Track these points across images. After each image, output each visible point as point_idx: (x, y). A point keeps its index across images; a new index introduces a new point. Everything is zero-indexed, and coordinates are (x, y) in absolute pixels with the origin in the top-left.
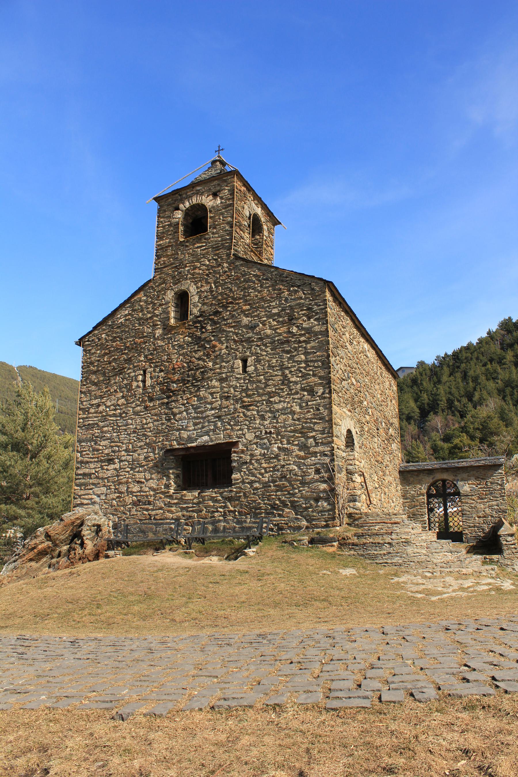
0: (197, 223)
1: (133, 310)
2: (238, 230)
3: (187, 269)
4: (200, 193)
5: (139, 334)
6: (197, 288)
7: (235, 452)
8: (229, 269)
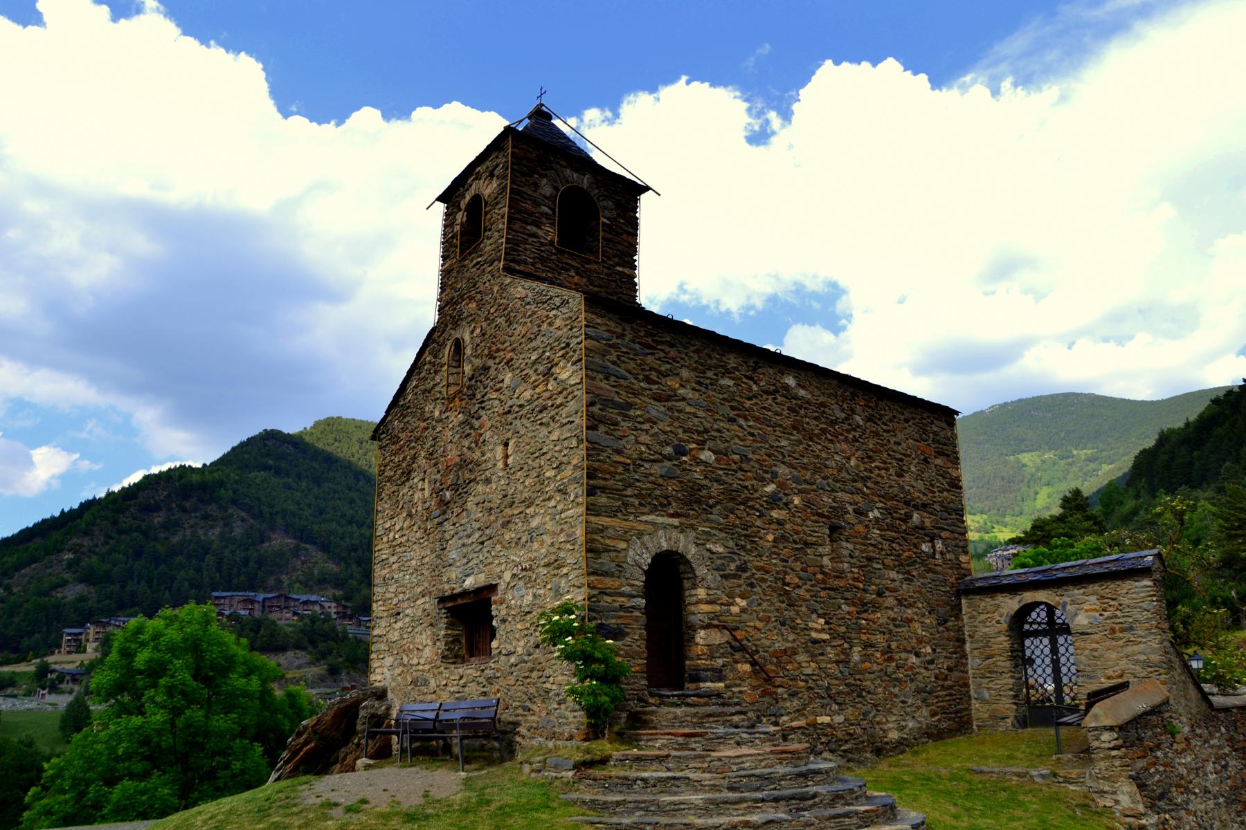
7: (495, 603)
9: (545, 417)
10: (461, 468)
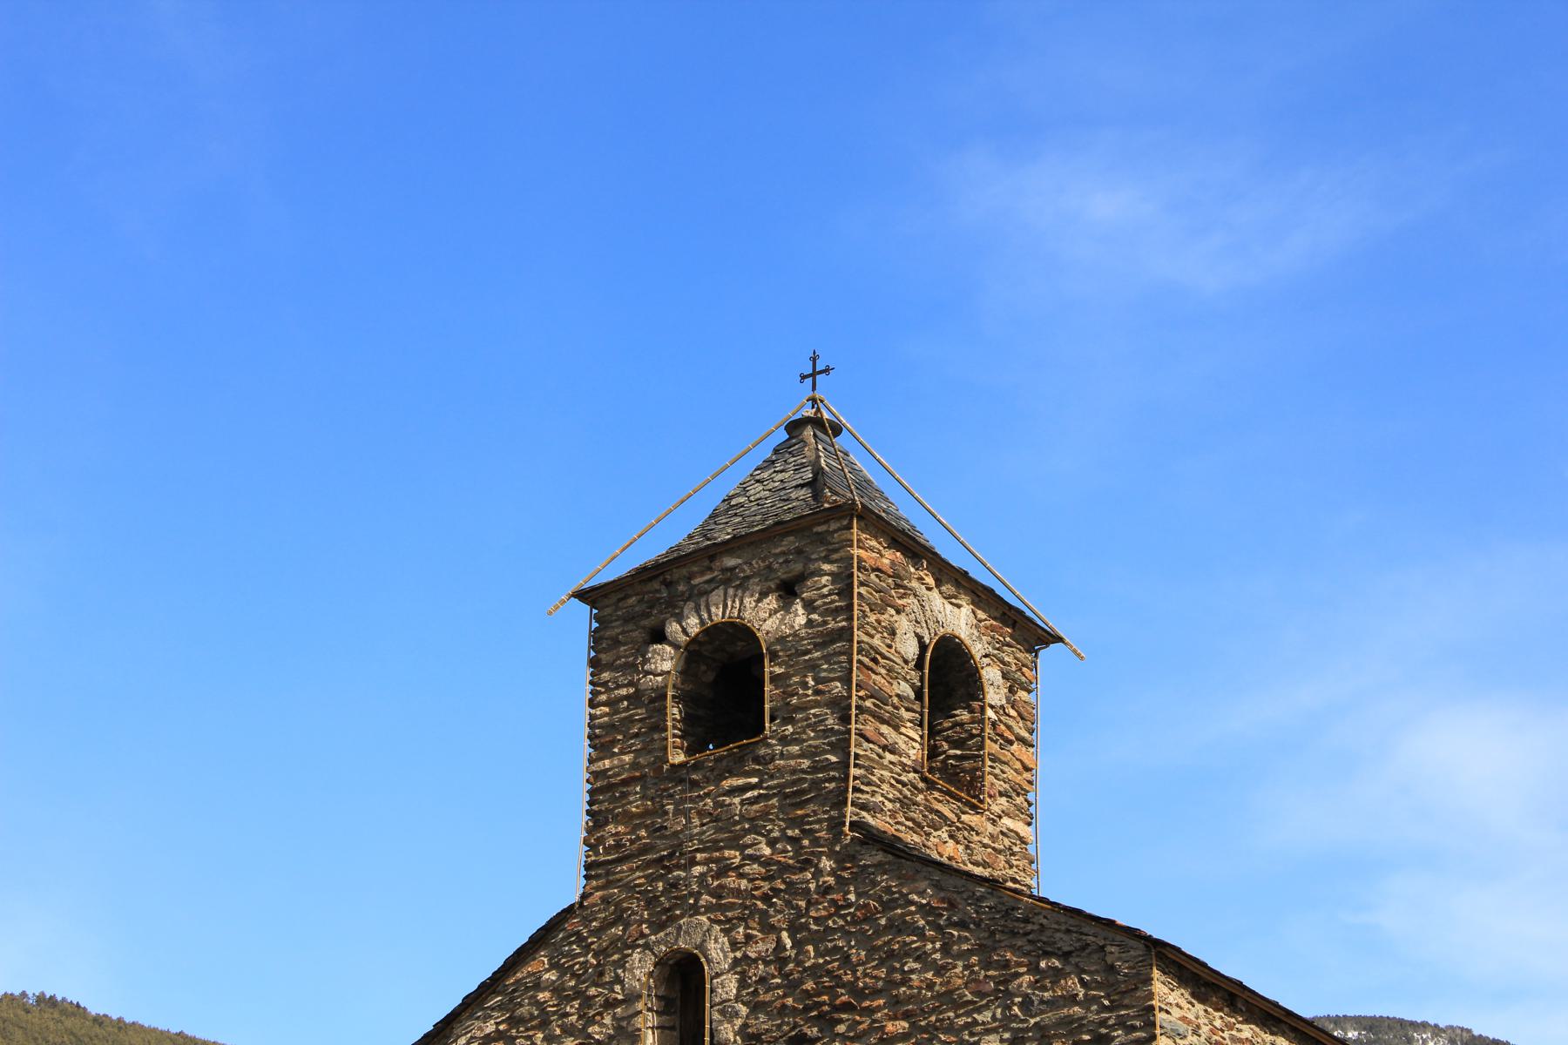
0: (728, 690)
1: (514, 1021)
2: (869, 729)
3: (697, 870)
4: (733, 581)
6: (734, 945)
8: (839, 879)
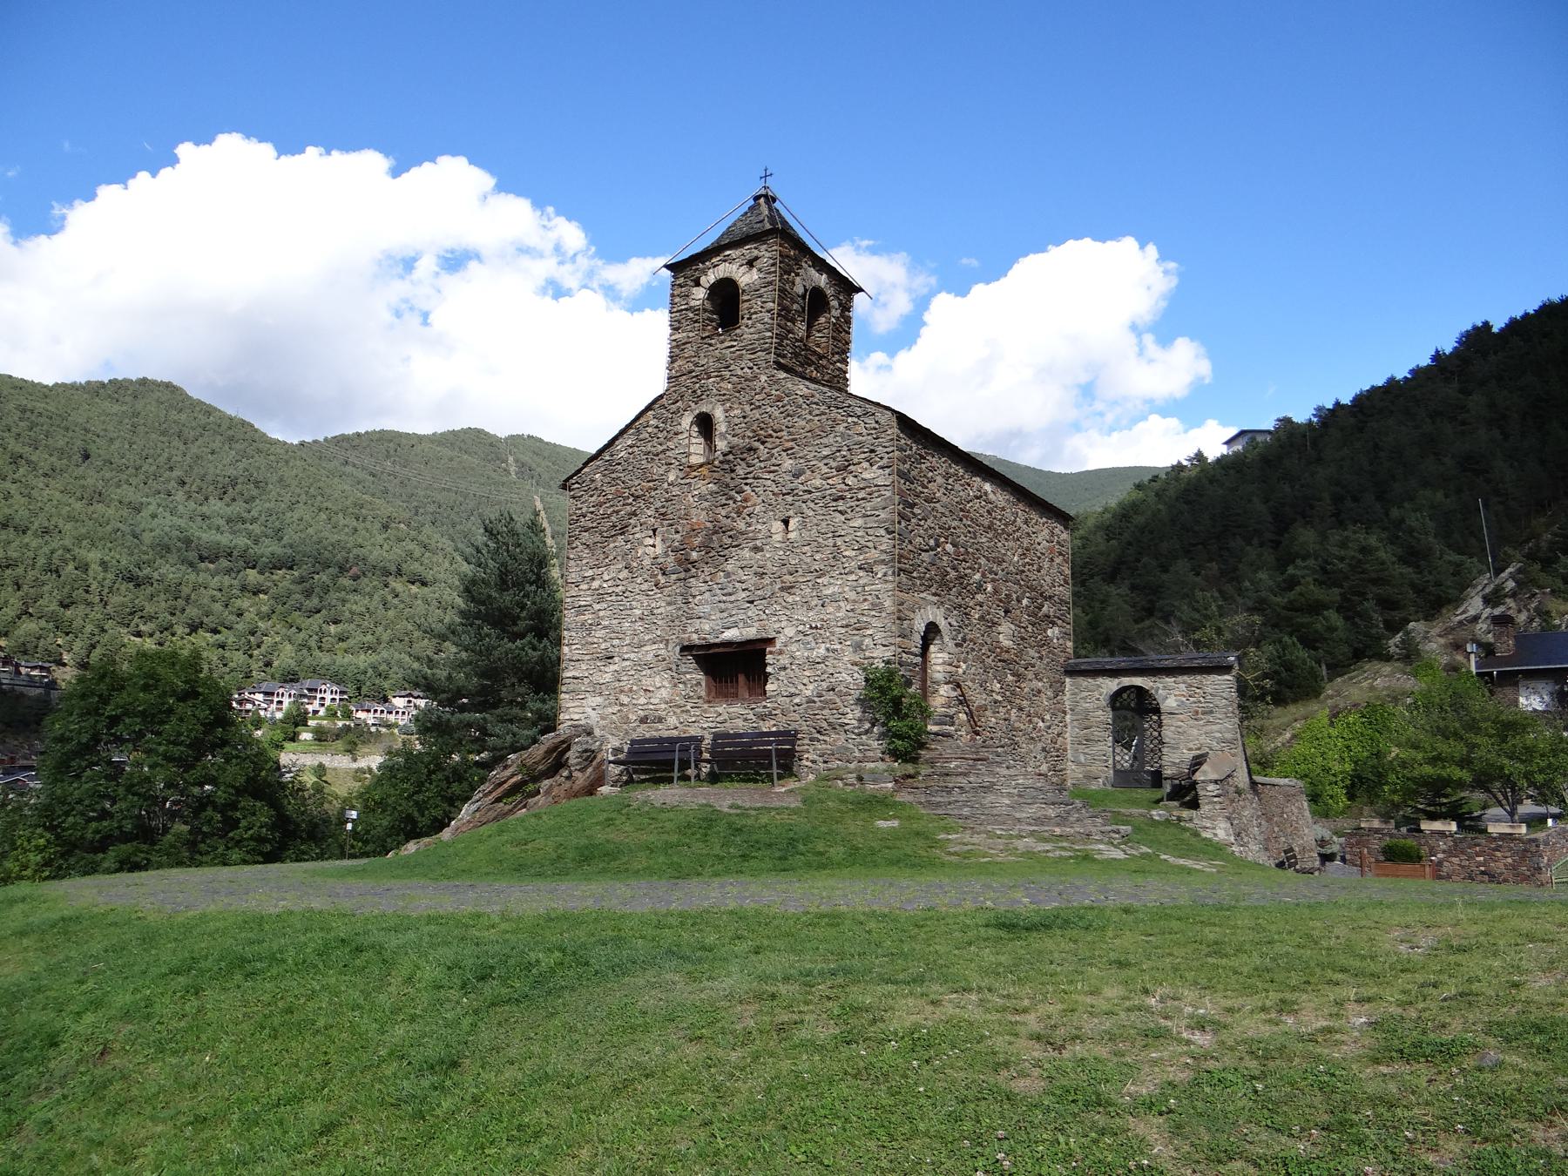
5: (645, 476)
9: (841, 505)
10: (716, 532)
